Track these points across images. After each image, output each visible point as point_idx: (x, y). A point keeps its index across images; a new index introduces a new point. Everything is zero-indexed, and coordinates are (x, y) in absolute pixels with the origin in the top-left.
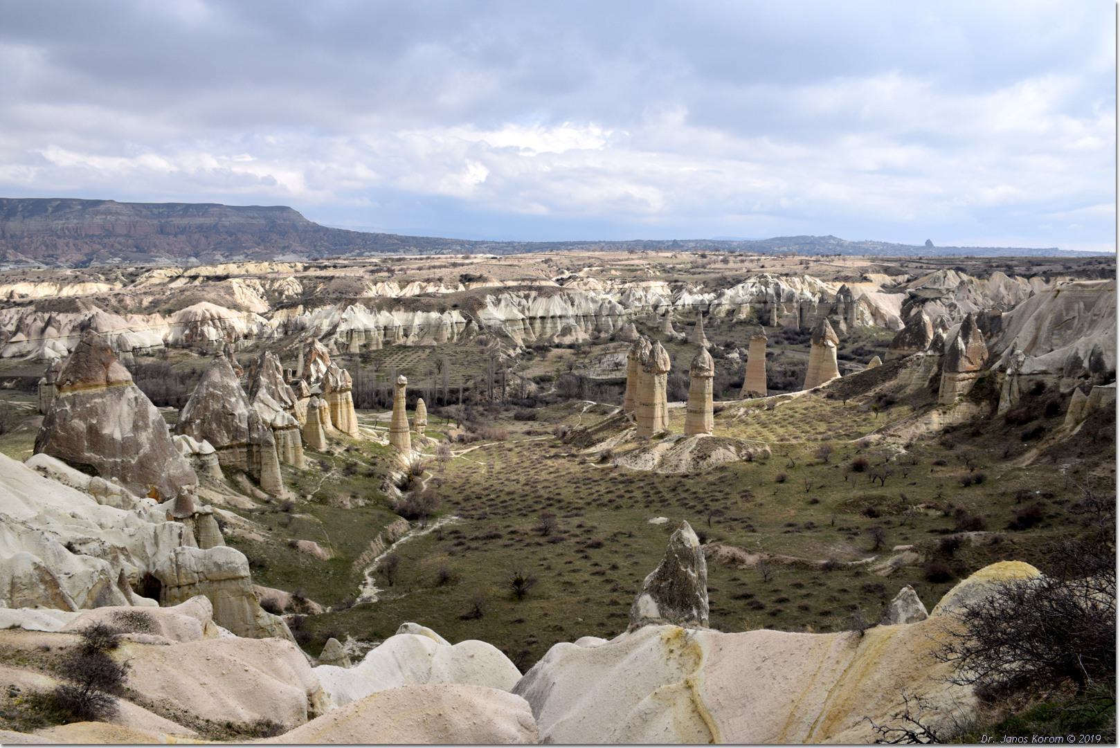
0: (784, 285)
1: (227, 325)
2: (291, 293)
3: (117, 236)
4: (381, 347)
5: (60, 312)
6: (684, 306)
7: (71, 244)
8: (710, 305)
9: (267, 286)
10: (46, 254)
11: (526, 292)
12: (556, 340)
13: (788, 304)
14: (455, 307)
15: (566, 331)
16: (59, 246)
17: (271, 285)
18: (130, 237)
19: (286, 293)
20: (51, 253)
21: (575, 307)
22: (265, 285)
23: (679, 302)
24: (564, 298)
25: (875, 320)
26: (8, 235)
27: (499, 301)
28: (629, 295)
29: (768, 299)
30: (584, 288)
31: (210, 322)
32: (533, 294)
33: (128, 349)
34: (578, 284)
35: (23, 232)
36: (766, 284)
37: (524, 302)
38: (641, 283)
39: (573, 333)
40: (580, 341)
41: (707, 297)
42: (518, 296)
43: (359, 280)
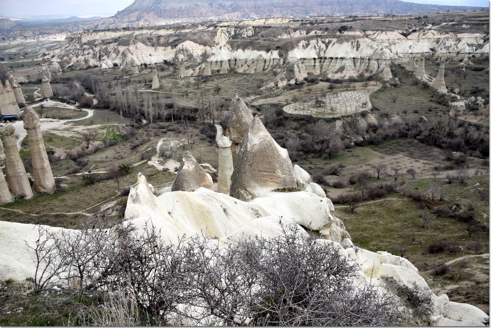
1: (189, 53)
2: (245, 36)
3: (298, 6)
4: (226, 72)
5: (124, 45)
7: (279, 11)
9: (237, 32)
10: (268, 15)
11: (330, 39)
12: (330, 76)
14: (278, 48)
15: (342, 69)
16: (274, 11)
17: (239, 31)
18: (304, 7)
19: (243, 36)
20: (270, 14)
21: (359, 51)
22: (236, 31)
24: (354, 44)
26: (257, 7)
27: (308, 45)
28: (440, 44)
30: (425, 37)
31: (182, 52)
32: (334, 40)
33: (199, 61)
34: (419, 34)
35: (262, 5)
37: (323, 46)
39: (344, 72)
40: (346, 78)
42: (323, 42)
43: (286, 29)
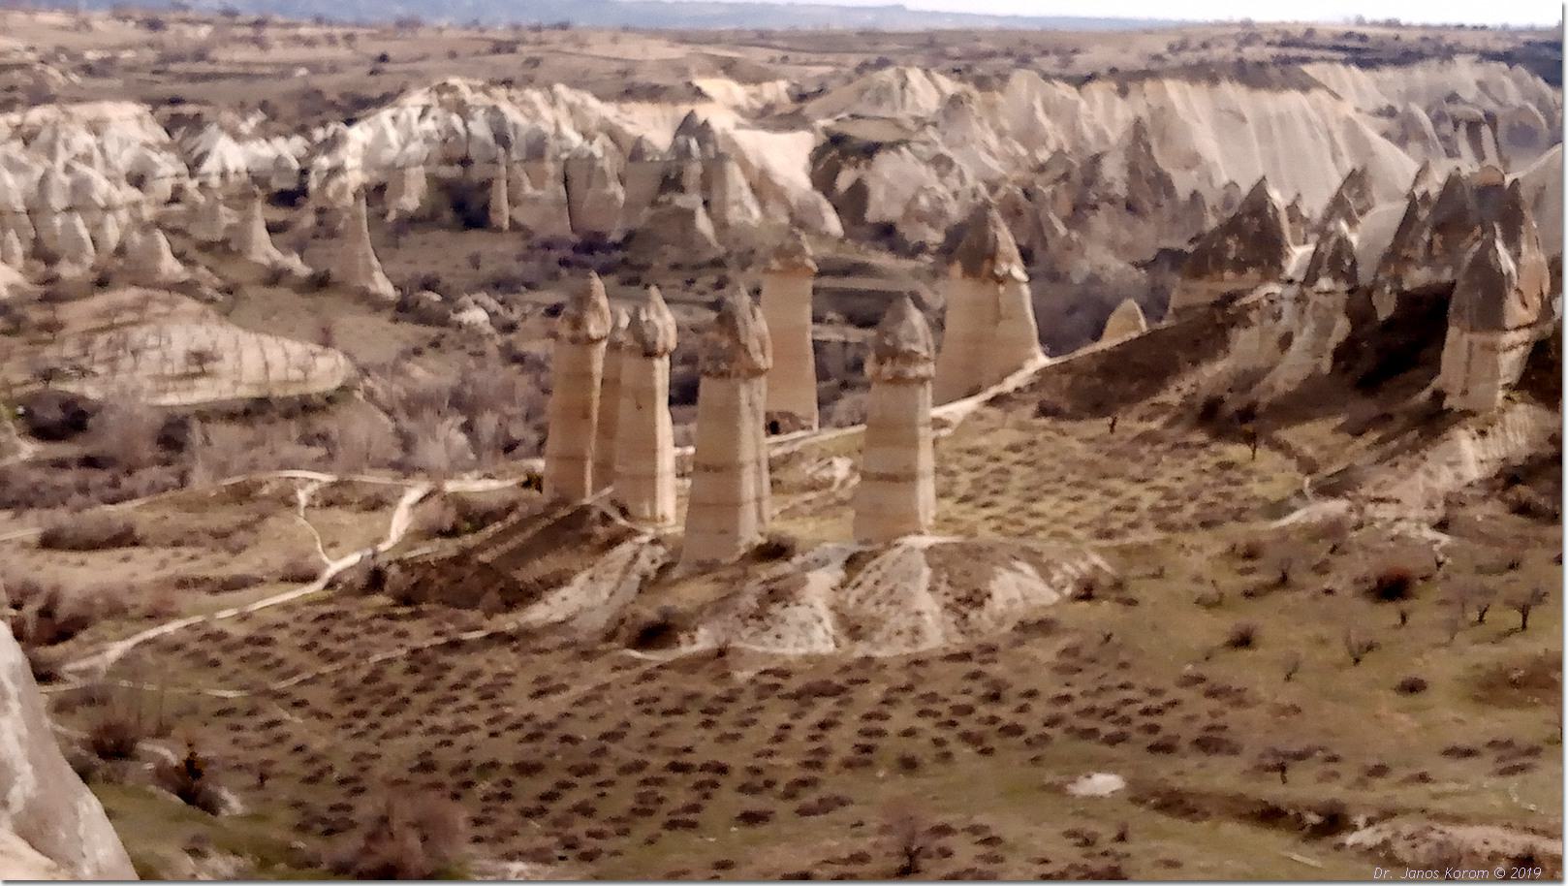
0: (513, 114)
6: (224, 175)
8: (304, 172)
13: (533, 165)
23: (210, 166)
25: (762, 205)
29: (473, 153)
36: (462, 109)
38: (76, 109)
41: (289, 149)
